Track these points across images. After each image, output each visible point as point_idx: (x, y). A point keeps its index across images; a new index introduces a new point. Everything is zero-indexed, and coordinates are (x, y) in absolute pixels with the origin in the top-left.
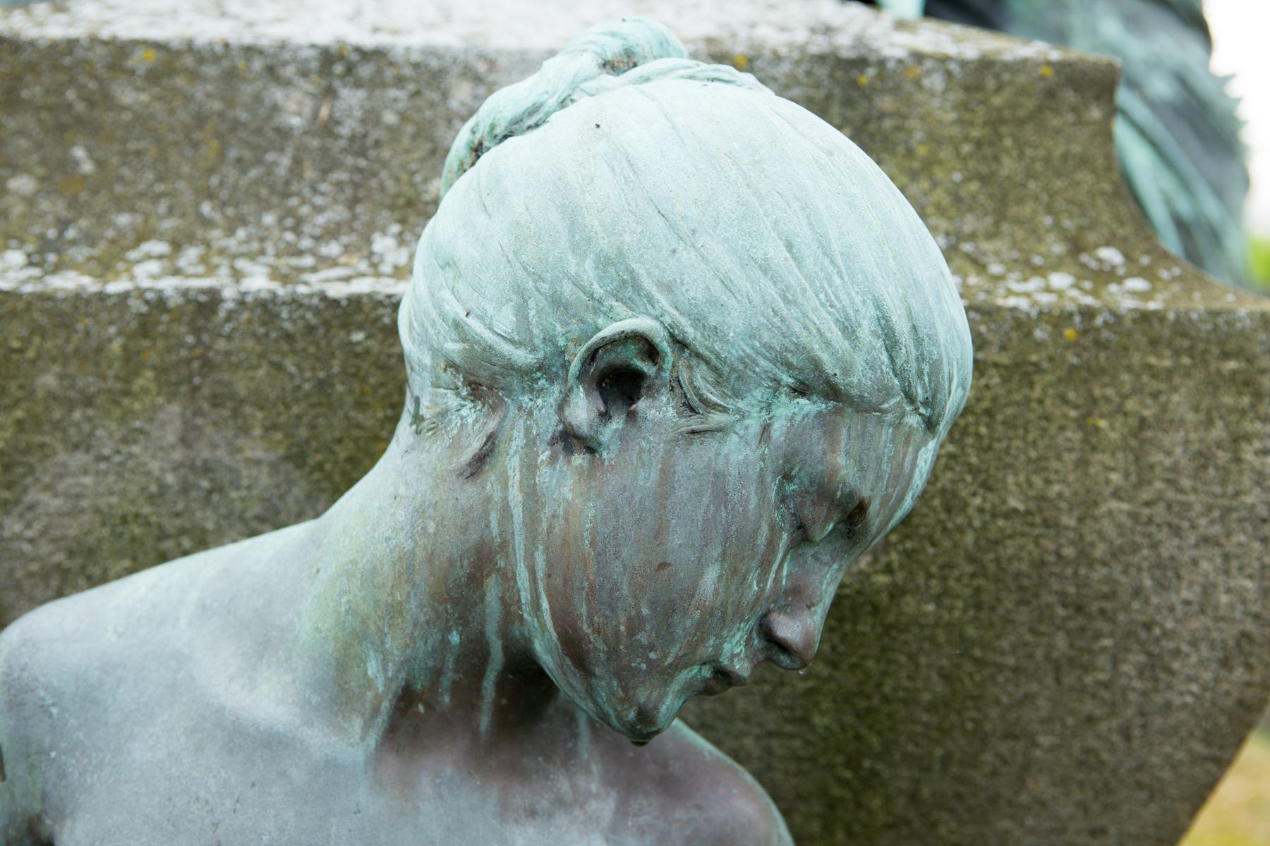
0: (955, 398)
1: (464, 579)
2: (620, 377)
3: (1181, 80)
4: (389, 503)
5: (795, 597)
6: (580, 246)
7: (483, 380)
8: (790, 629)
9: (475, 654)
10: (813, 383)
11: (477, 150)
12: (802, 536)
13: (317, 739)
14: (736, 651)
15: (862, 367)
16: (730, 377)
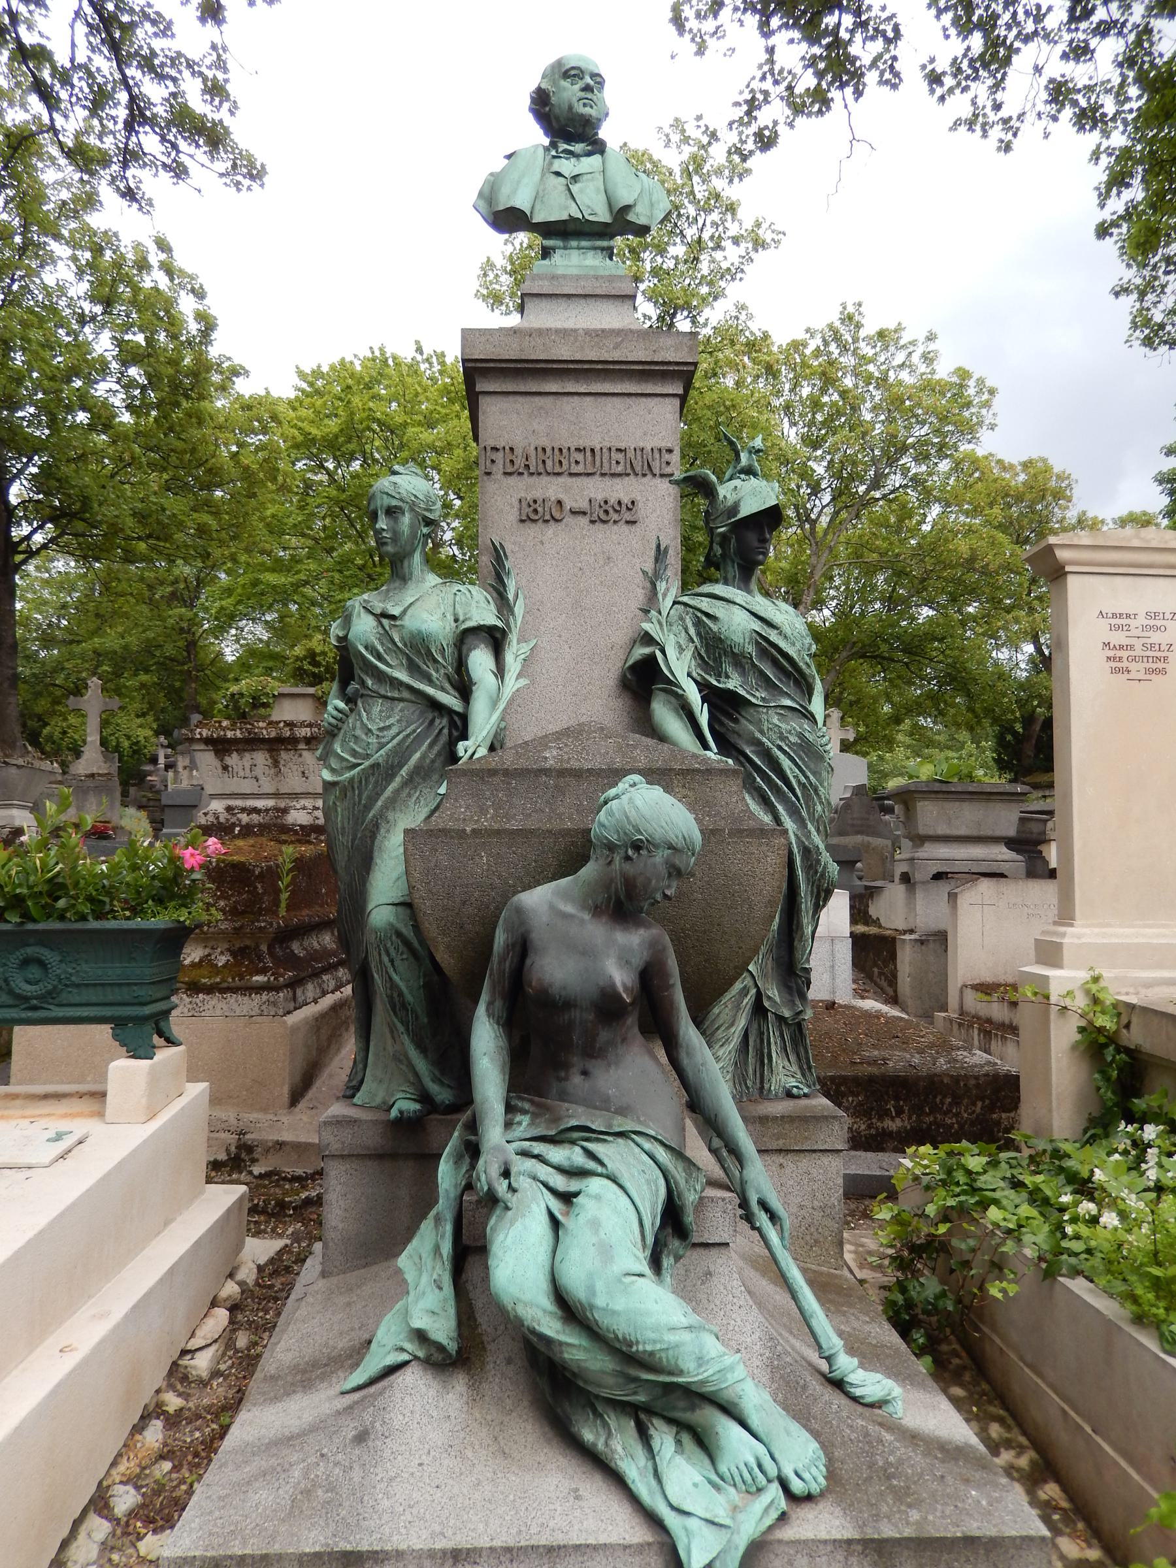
0: (698, 849)
1: (606, 884)
2: (637, 846)
3: (801, 736)
4: (589, 871)
5: (669, 887)
6: (629, 822)
7: (611, 847)
8: (668, 892)
9: (609, 898)
10: (671, 847)
11: (606, 803)
12: (670, 875)
13: (580, 914)
14: (659, 897)
15: (680, 844)
16: (656, 846)
